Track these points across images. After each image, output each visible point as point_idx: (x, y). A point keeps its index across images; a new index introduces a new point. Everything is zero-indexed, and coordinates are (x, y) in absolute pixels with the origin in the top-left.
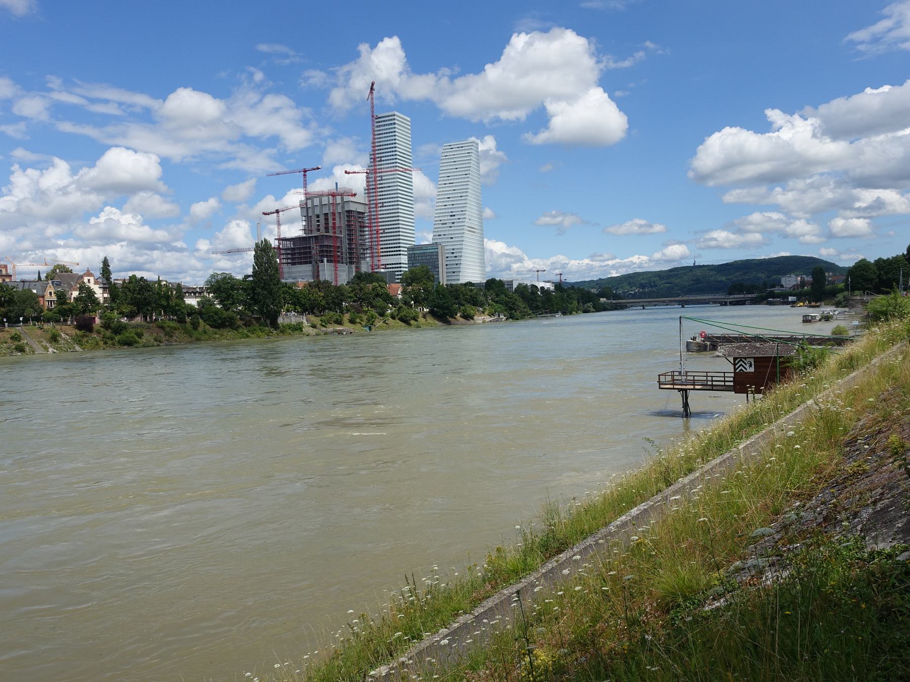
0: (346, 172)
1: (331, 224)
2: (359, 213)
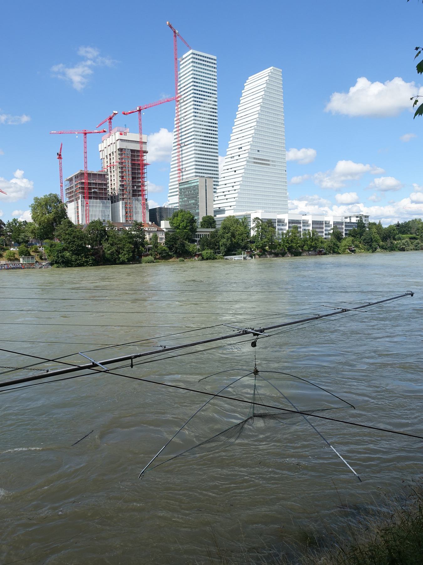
2: (133, 151)
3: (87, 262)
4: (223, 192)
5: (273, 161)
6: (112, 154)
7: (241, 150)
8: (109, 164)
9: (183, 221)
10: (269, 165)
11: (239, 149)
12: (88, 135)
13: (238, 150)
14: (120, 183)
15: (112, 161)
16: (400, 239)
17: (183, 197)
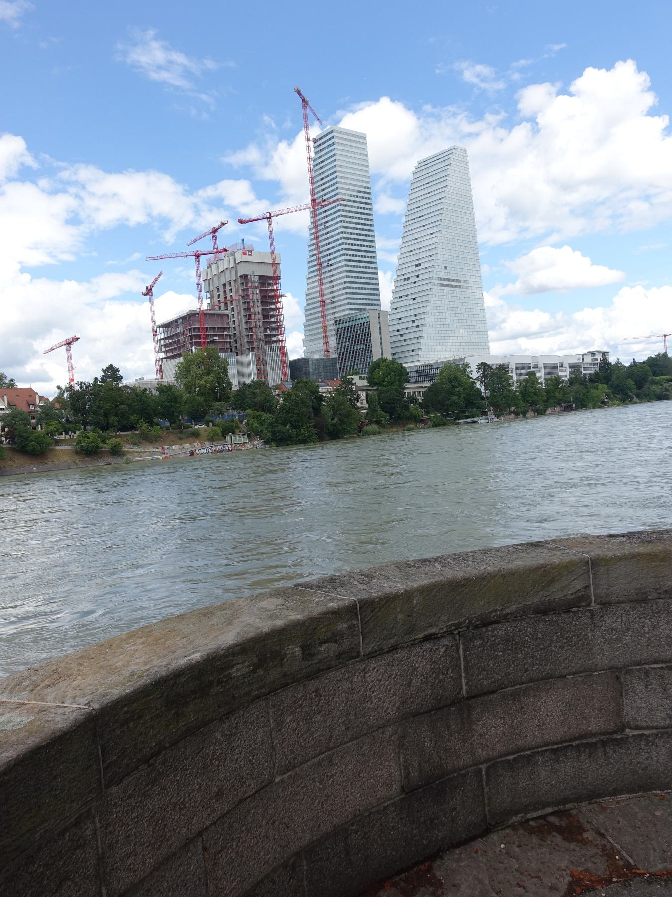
0: (241, 222)
1: (229, 298)
2: (261, 277)
3: (309, 436)
4: (398, 331)
5: (465, 282)
6: (227, 285)
7: (419, 268)
8: (222, 299)
9: (389, 374)
10: (460, 287)
11: (416, 266)
12: (201, 257)
13: (414, 268)
14: (245, 327)
15: (229, 294)
16: (654, 383)
17: (343, 340)
